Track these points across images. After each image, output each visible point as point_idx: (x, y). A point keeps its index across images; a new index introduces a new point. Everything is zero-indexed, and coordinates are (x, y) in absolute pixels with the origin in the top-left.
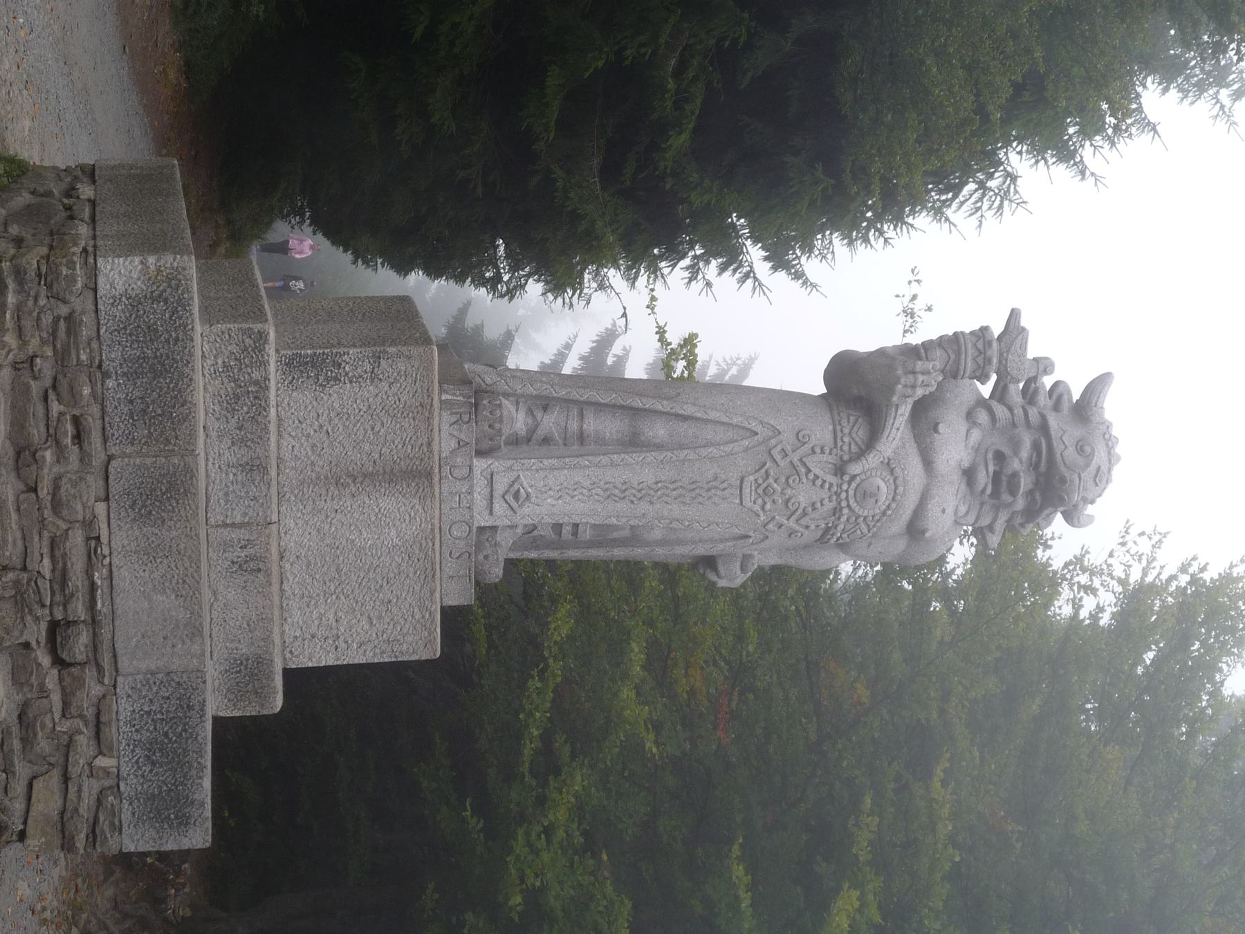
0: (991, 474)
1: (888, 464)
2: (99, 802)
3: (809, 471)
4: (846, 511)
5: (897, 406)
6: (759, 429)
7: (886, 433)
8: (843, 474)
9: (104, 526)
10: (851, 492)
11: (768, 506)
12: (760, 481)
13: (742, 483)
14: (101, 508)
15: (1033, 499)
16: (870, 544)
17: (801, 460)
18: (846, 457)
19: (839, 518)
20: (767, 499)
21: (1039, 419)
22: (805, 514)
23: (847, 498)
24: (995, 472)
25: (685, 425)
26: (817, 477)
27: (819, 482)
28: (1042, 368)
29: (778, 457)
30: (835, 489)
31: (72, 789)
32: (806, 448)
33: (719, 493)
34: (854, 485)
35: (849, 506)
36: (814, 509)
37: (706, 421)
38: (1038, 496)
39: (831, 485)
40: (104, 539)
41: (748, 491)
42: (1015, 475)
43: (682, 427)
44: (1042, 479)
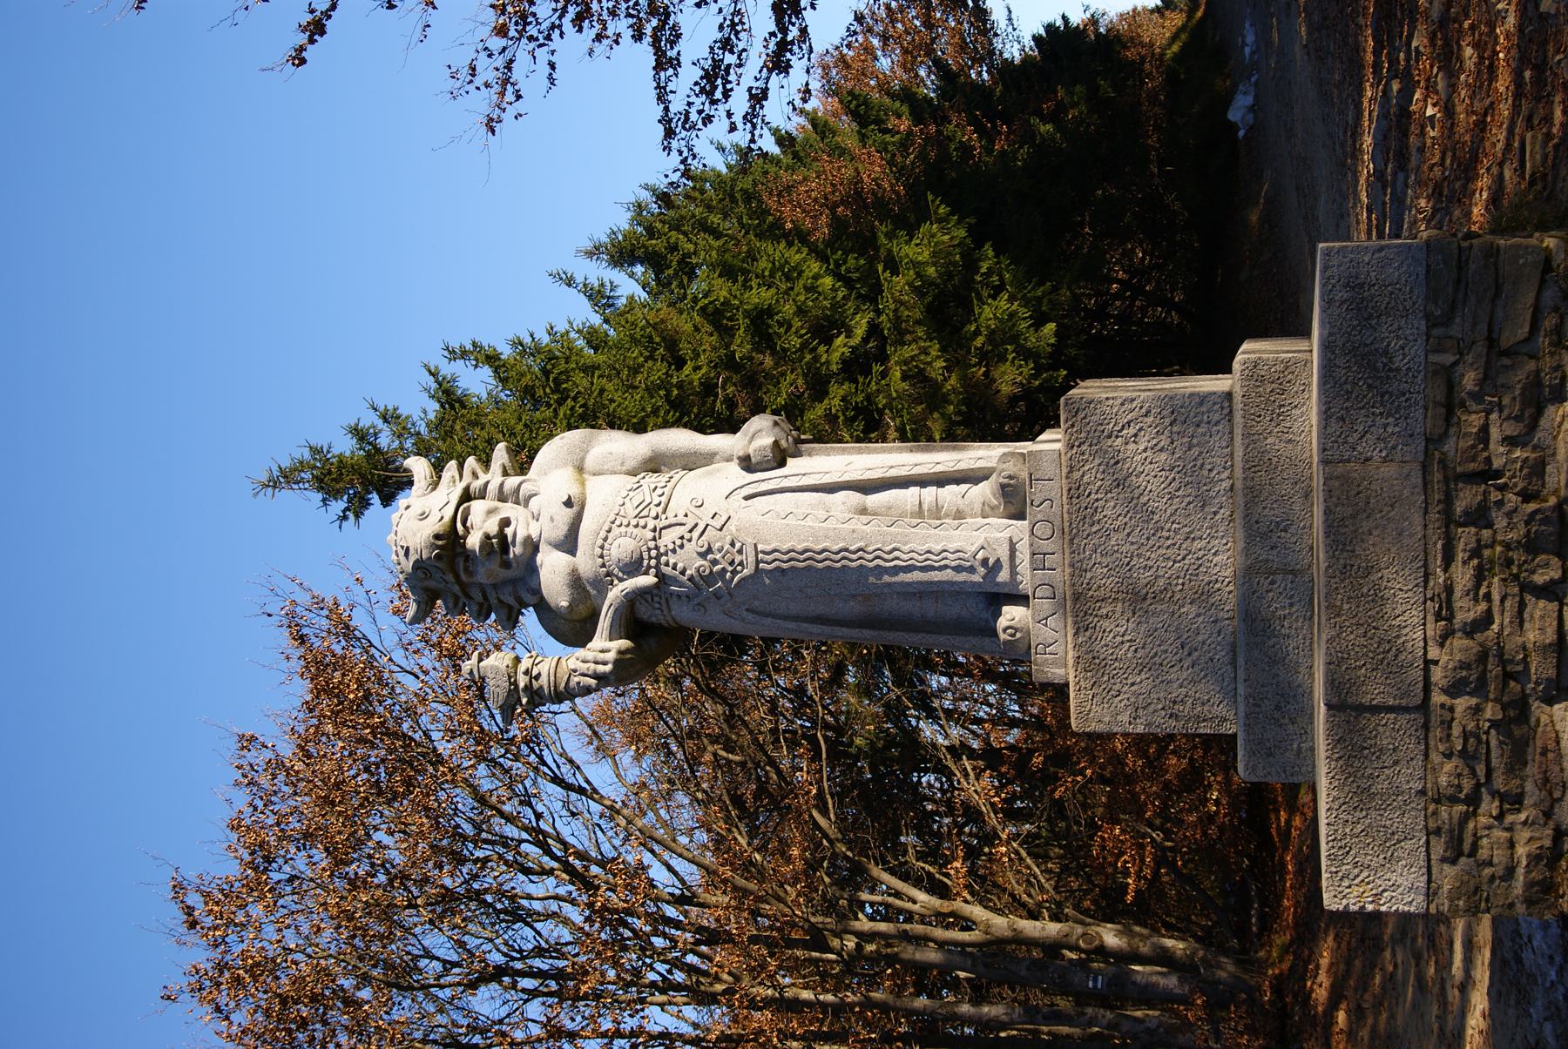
2: (1453, 308)
6: (745, 613)
9: (1430, 633)
14: (1433, 653)
15: (464, 523)
31: (1483, 328)
37: (796, 618)
40: (1430, 618)
43: (821, 609)
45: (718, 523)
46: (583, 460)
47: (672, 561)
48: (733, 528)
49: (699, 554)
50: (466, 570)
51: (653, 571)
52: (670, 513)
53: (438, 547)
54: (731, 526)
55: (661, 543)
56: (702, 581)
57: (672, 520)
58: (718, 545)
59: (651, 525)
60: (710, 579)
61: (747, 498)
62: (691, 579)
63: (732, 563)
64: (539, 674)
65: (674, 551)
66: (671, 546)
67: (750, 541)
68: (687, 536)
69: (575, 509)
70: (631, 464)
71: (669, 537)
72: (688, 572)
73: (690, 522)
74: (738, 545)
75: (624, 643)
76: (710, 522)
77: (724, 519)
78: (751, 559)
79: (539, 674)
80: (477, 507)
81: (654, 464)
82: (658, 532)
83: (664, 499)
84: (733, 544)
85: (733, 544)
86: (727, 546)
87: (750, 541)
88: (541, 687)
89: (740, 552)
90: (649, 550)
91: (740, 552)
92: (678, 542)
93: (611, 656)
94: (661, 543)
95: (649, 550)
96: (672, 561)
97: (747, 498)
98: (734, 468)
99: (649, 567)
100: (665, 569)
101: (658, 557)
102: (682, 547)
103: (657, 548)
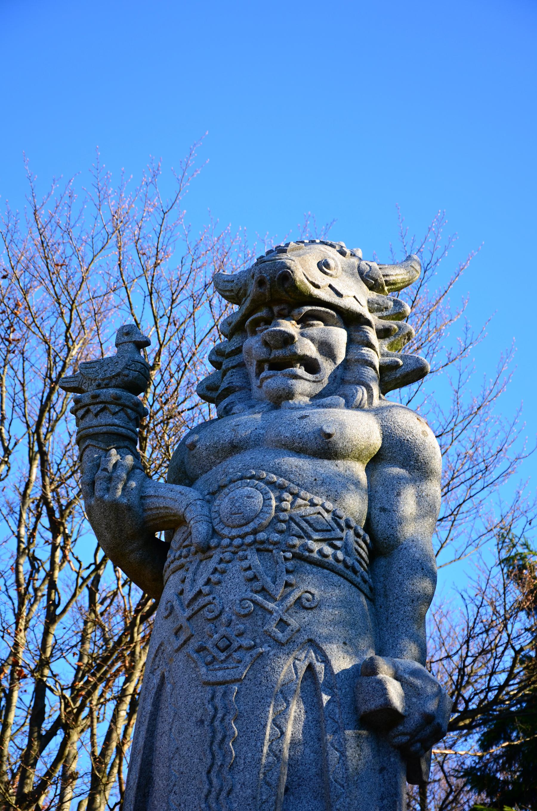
0: (272, 372)
1: (213, 494)
3: (200, 592)
4: (262, 536)
5: (142, 498)
6: (159, 672)
7: (169, 504)
8: (209, 548)
10: (234, 532)
11: (246, 642)
12: (209, 659)
13: (207, 683)
17: (189, 606)
18: (193, 549)
19: (275, 543)
20: (236, 645)
21: (234, 338)
22: (263, 591)
23: (242, 537)
24: (270, 369)
25: (157, 779)
26: (208, 582)
27: (215, 578)
28: (126, 338)
29: (183, 637)
30: (227, 556)
32: (176, 603)
33: (220, 715)
34: (226, 531)
35: (255, 532)
36: (255, 578)
39: (221, 561)
41: (220, 673)
42: (266, 344)
43: (160, 783)
44: (276, 309)
50: (256, 323)
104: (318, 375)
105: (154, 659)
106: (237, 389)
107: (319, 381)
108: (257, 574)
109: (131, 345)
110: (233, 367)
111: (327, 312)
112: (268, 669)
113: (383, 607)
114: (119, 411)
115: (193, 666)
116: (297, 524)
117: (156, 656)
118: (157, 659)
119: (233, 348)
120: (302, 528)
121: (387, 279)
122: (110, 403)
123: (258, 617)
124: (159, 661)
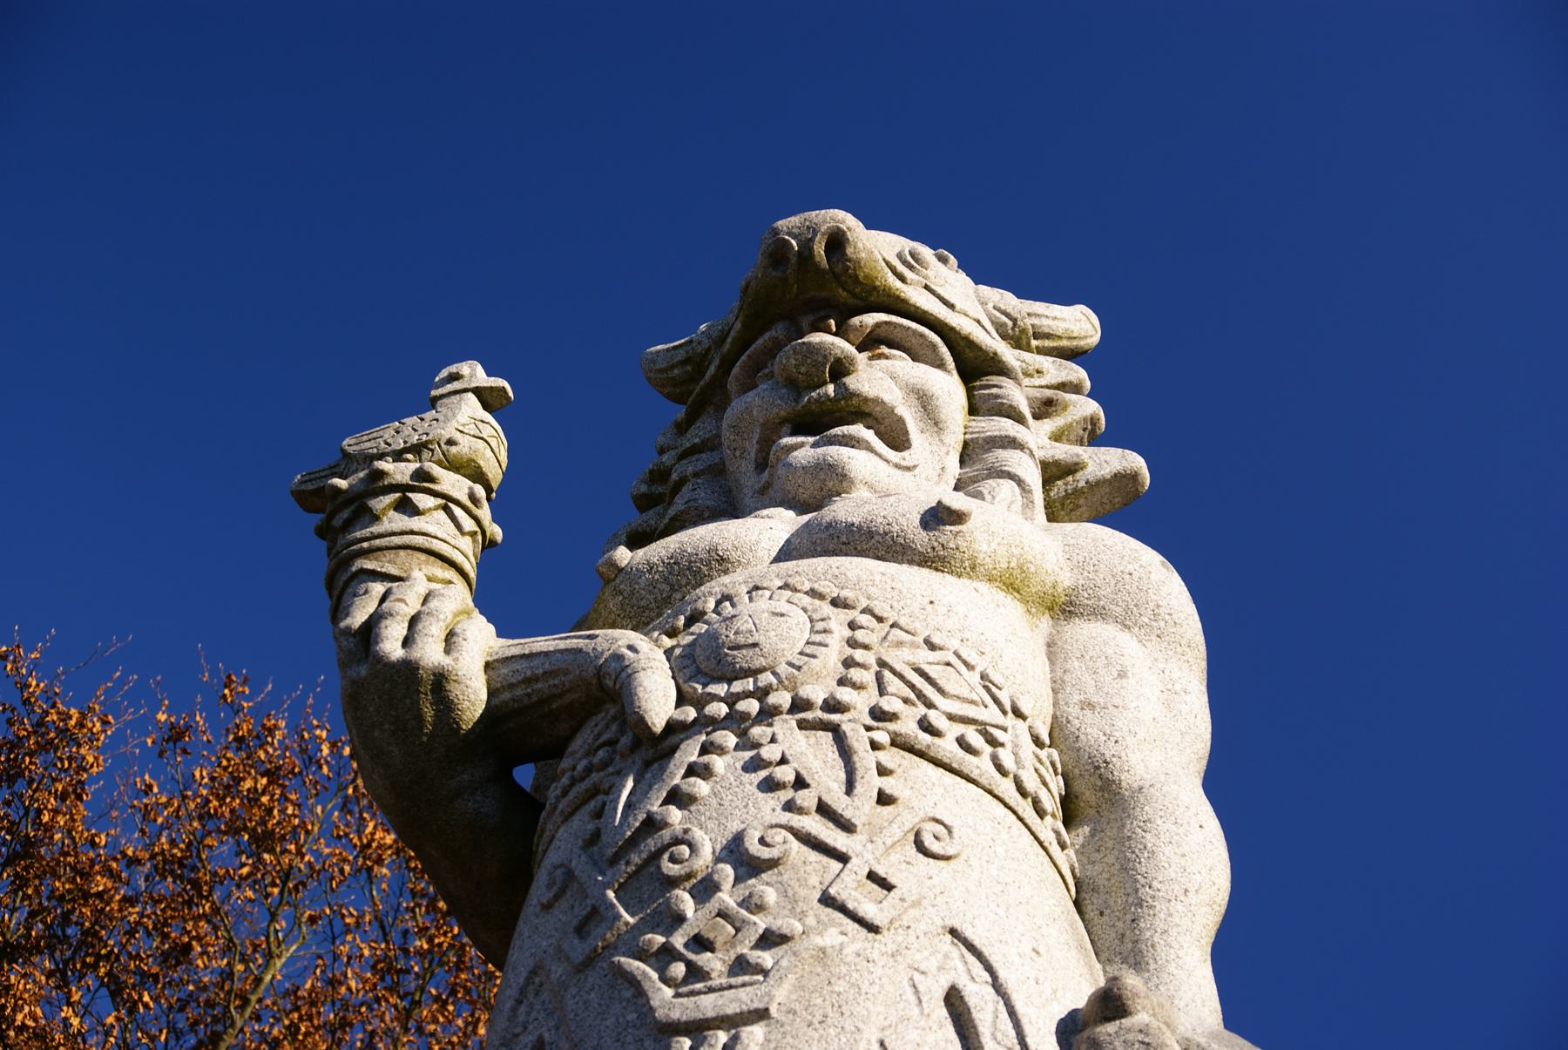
16: (1088, 705)
38: (871, 319)
45: (852, 889)
46: (1098, 613)
47: (718, 763)
48: (831, 938)
49: (738, 838)
51: (690, 713)
52: (890, 757)
53: (807, 245)
54: (835, 933)
55: (785, 726)
56: (649, 874)
57: (866, 760)
58: (771, 896)
59: (860, 702)
60: (651, 887)
61: (955, 1002)
62: (652, 824)
63: (701, 943)
64: (414, 511)
65: (754, 765)
66: (770, 753)
67: (779, 995)
68: (806, 798)
69: (920, 538)
70: (1090, 729)
71: (810, 754)
72: (675, 815)
73: (859, 808)
74: (766, 958)
75: (473, 696)
76: (859, 867)
77: (868, 910)
78: (708, 1005)
79: (414, 511)
80: (948, 387)
81: (1090, 800)
82: (825, 720)
83: (947, 747)
84: (769, 940)
85: (769, 940)
86: (761, 923)
87: (779, 995)
88: (376, 518)
89: (741, 966)
90: (762, 693)
91: (741, 966)
92: (786, 774)
93: (430, 653)
94: (785, 726)
95: (762, 693)
96: (718, 763)
97: (955, 1002)
98: (1078, 992)
99: (700, 703)
100: (689, 752)
101: (737, 722)
102: (770, 785)
103: (768, 714)
104: (905, 454)
105: (514, 1010)
106: (706, 515)
107: (908, 469)
108: (804, 773)
109: (470, 395)
110: (696, 475)
111: (922, 335)
112: (840, 986)
113: (1107, 912)
114: (436, 508)
115: (628, 994)
116: (901, 677)
117: (519, 1002)
118: (523, 1008)
119: (697, 440)
120: (912, 687)
121: (1036, 321)
122: (414, 489)
123: (808, 868)
124: (528, 1013)
